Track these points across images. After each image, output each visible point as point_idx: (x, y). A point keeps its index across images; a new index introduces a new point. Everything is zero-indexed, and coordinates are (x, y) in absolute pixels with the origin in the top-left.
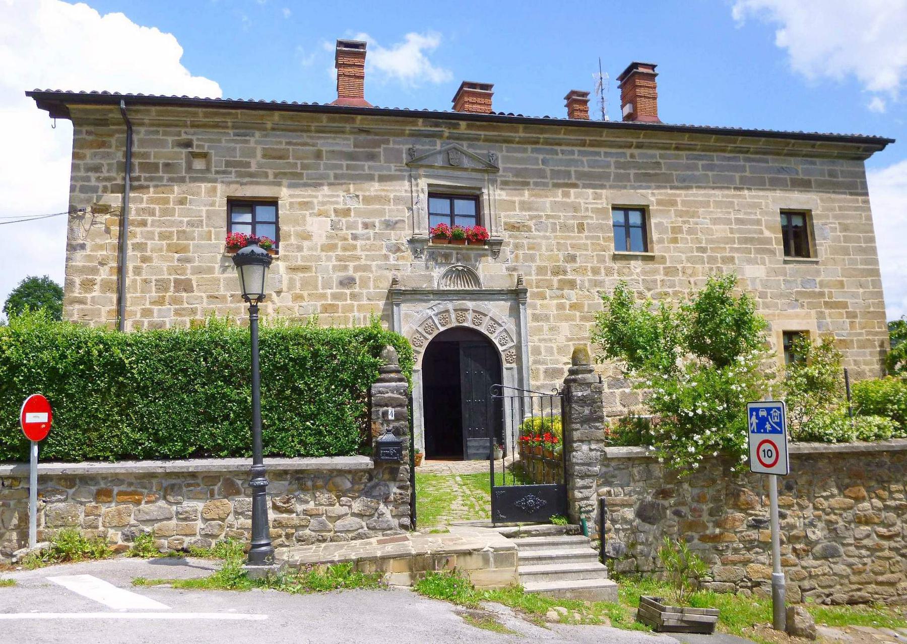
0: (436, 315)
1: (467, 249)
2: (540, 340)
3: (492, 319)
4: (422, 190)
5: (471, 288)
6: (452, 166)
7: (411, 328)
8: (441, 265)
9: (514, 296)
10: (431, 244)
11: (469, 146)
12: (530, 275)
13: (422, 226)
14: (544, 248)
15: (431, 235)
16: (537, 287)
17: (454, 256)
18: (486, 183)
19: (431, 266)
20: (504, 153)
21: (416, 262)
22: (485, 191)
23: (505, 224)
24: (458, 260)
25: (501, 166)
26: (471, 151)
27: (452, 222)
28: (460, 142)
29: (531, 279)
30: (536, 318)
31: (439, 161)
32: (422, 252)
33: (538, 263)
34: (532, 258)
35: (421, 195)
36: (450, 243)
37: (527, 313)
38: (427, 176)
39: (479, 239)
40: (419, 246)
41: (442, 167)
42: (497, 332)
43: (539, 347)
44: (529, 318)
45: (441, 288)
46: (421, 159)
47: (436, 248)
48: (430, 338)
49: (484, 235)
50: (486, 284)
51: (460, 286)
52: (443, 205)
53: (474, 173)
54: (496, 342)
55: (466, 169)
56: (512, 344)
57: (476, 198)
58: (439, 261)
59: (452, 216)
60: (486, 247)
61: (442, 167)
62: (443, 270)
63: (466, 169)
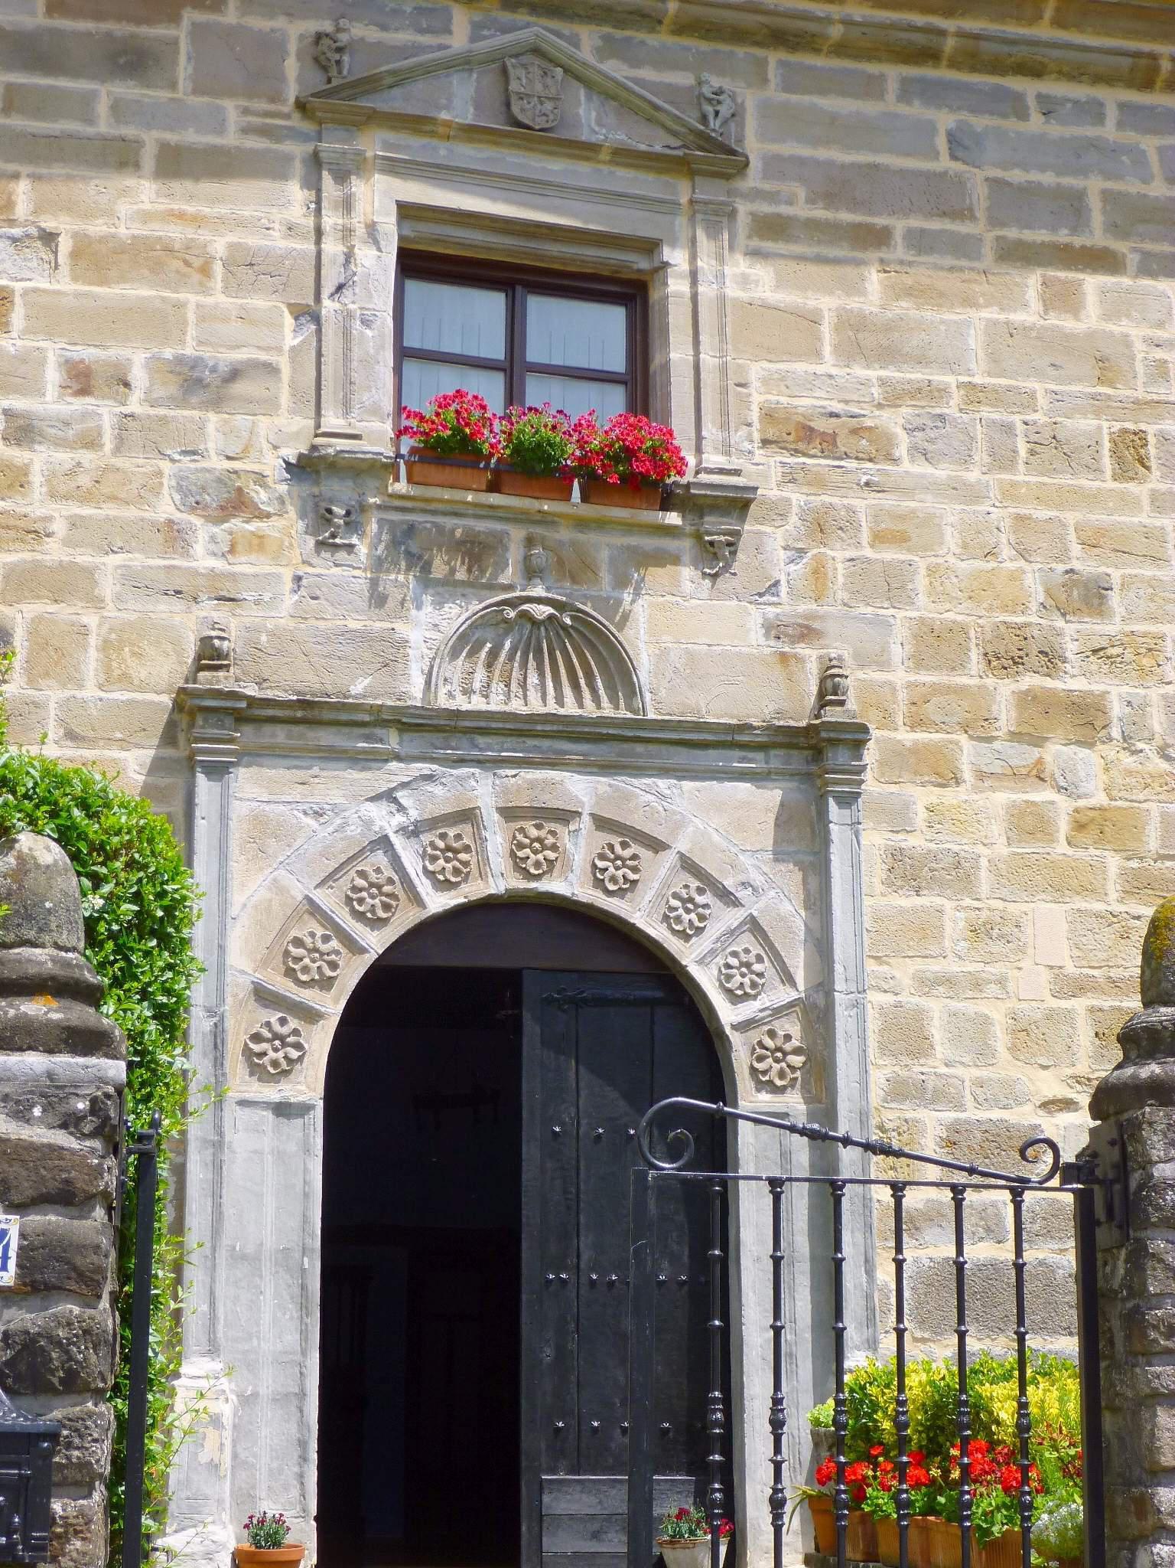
0: (412, 832)
1: (582, 524)
2: (927, 984)
3: (687, 864)
4: (372, 229)
5: (590, 710)
6: (518, 130)
7: (278, 887)
8: (447, 588)
9: (798, 760)
10: (402, 487)
11: (610, 48)
12: (884, 665)
13: (363, 397)
14: (951, 540)
15: (407, 444)
16: (917, 723)
17: (514, 554)
18: (681, 222)
19: (395, 595)
20: (773, 92)
21: (326, 569)
22: (676, 257)
23: (769, 415)
24: (531, 573)
25: (754, 146)
26: (615, 69)
27: (513, 394)
28: (565, 27)
29: (884, 683)
30: (907, 871)
31: (461, 101)
32: (353, 524)
33: (924, 607)
34: (893, 586)
35: (366, 255)
36: (494, 487)
37: (860, 845)
38: (394, 167)
39: (636, 474)
40: (340, 492)
41: (471, 133)
42: (714, 929)
43: (919, 1016)
44: (875, 872)
45: (443, 702)
46: (370, 84)
47: (427, 507)
48: (376, 942)
49: (665, 458)
50: (662, 695)
51: (535, 697)
53: (621, 172)
54: (706, 979)
55: (585, 150)
56: (784, 995)
58: (439, 569)
59: (514, 368)
60: (673, 518)
61: (471, 133)
62: (456, 615)
63: (585, 150)
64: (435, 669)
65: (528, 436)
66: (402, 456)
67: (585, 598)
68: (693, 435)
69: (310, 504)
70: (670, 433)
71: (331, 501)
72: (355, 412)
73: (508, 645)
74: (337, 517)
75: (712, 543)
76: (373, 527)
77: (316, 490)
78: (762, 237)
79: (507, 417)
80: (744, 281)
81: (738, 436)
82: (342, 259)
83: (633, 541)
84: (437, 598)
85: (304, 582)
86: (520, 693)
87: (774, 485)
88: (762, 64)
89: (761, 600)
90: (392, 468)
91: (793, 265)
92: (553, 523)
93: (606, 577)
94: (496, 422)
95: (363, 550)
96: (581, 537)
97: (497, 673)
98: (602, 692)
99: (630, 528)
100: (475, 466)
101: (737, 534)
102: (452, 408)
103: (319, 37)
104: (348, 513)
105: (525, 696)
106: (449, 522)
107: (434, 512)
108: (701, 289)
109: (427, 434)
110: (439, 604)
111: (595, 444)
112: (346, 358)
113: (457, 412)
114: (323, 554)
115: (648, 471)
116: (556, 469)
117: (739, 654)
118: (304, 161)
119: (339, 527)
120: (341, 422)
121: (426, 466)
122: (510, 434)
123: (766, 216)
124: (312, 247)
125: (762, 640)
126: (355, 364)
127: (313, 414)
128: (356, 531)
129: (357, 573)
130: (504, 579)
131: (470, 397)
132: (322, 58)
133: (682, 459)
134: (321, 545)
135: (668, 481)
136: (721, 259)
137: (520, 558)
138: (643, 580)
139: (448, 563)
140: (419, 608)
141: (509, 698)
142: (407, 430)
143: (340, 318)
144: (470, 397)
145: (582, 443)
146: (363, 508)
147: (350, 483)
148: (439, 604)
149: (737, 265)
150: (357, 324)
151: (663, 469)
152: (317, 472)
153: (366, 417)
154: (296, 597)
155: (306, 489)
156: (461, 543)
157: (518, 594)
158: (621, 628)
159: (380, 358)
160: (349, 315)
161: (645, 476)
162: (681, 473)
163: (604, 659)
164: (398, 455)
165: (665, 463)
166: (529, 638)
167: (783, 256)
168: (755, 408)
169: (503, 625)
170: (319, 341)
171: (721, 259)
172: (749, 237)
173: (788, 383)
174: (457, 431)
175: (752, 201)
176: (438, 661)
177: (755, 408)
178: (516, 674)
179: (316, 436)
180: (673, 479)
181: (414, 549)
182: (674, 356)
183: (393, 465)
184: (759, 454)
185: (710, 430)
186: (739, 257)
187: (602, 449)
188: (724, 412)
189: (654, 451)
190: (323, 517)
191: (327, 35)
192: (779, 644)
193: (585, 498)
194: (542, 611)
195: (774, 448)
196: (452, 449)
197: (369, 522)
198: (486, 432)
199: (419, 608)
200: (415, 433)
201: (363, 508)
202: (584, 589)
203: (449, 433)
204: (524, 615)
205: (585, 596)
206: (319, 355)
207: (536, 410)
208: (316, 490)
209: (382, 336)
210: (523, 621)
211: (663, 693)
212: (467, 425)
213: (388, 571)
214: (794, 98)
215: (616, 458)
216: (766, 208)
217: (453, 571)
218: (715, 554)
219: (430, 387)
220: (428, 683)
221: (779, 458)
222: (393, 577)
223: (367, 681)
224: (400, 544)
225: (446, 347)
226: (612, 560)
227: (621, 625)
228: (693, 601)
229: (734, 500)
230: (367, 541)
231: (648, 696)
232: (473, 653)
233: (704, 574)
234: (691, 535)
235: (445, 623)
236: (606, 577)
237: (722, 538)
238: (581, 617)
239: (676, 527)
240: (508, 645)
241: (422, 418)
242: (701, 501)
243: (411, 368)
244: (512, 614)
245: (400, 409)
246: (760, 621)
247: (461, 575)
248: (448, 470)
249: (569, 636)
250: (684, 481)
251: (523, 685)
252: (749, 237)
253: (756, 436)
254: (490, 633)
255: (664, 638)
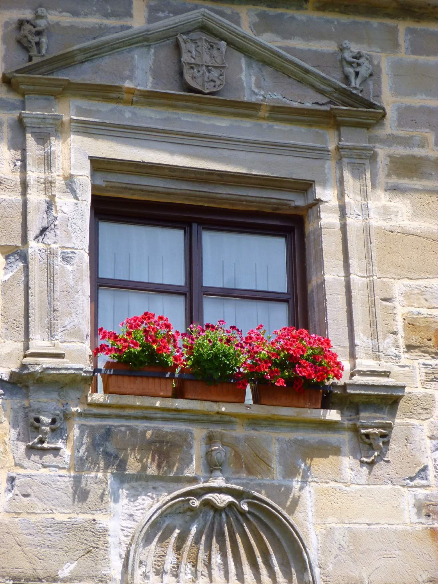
1: (254, 422)
4: (69, 181)
6: (190, 96)
8: (140, 483)
10: (99, 397)
11: (265, 24)
13: (65, 322)
15: (103, 359)
17: (197, 450)
18: (330, 165)
19: (95, 490)
20: (404, 55)
21: (36, 470)
22: (326, 194)
23: (411, 325)
24: (212, 466)
25: (389, 100)
26: (270, 40)
27: (193, 315)
28: (228, 9)
31: (142, 72)
32: (58, 430)
35: (64, 202)
36: (178, 393)
38: (86, 129)
39: (299, 381)
40: (47, 404)
41: (150, 98)
46: (65, 61)
47: (121, 412)
49: (324, 362)
52: (155, 253)
53: (278, 126)
55: (247, 109)
57: (289, 223)
58: (133, 467)
59: (192, 292)
60: (333, 415)
61: (150, 98)
62: (148, 505)
63: (247, 109)
64: (132, 554)
65: (206, 349)
66: (99, 371)
67: (260, 487)
68: (347, 343)
69: (21, 414)
70: (328, 342)
71: (39, 411)
72: (59, 335)
73: (194, 530)
74: (44, 425)
75: (367, 436)
76: (76, 432)
77: (26, 403)
78: (399, 176)
79: (188, 334)
80: (385, 212)
81: (386, 343)
82: (44, 206)
83: (300, 435)
84: (133, 492)
85: (17, 482)
86: (206, 572)
87: (418, 384)
88: (394, 31)
89: (412, 483)
90: (89, 381)
91: (426, 198)
92: (230, 422)
93: (277, 467)
94: (179, 339)
95: (66, 452)
96: (254, 433)
97: (185, 555)
98: (277, 568)
99: (297, 424)
100: (162, 377)
101: (389, 427)
102: (141, 328)
103: (21, 23)
104: (54, 421)
105: (210, 575)
106: (140, 425)
107: (128, 417)
108: (349, 221)
109: (120, 351)
110: (133, 497)
111: (264, 354)
112: (50, 289)
113: (146, 331)
114: (33, 457)
115: (310, 375)
116: (231, 376)
117: (395, 532)
118: (10, 126)
119: (46, 433)
120: (47, 343)
121: (120, 378)
122: (191, 348)
123: (402, 157)
124: (19, 198)
125: (415, 519)
126: (57, 295)
127: (22, 338)
128: (61, 437)
129: (63, 472)
130: (189, 473)
131: (156, 318)
132: (24, 40)
133: (339, 364)
134: (31, 449)
135: (328, 383)
136: (365, 196)
137: (202, 453)
138: (309, 469)
139: (140, 461)
140: (116, 500)
141: (196, 577)
142: (103, 348)
143: (44, 256)
144: (156, 318)
145: (252, 353)
146: (67, 416)
147: (55, 395)
148: (133, 497)
149: (379, 199)
150: (59, 261)
151: (324, 373)
152: (27, 387)
153: (67, 339)
154: (10, 495)
155: (17, 402)
156: (151, 442)
157: (201, 485)
158: (291, 511)
159: (79, 288)
160: (52, 254)
161: (307, 380)
162: (338, 376)
163: (278, 540)
164: (96, 370)
165: (324, 368)
166: (212, 524)
167: (417, 191)
168: (399, 319)
169: (189, 513)
170: (27, 276)
171: (365, 196)
172: (388, 175)
173: (427, 296)
174: (146, 347)
175: (389, 146)
176: (133, 546)
177: (399, 319)
178: (202, 555)
179: (25, 356)
180: (331, 381)
181: (111, 448)
182: (327, 277)
183: (91, 378)
184: (405, 358)
185: (361, 339)
186: (380, 193)
187: (270, 358)
188: (373, 323)
189: (314, 358)
190: (32, 425)
191: (28, 22)
192: (430, 522)
193: (256, 400)
194: (222, 500)
195: (417, 353)
196: (142, 363)
197: (71, 428)
198: (171, 347)
199: (116, 500)
200: (110, 350)
201: (67, 416)
202: (258, 479)
203: (139, 349)
204: (208, 504)
205: (260, 485)
206: (27, 287)
207: (213, 327)
208: (26, 403)
209: (80, 270)
210: (207, 509)
211: (330, 567)
212: (155, 341)
213: (89, 470)
214: (422, 59)
215: (282, 366)
216: (401, 151)
217: (144, 468)
218: (371, 445)
219: (121, 312)
220: (126, 566)
221: (422, 361)
222: (93, 474)
223: (73, 566)
224: (99, 445)
225: (135, 277)
226: (282, 452)
227: (292, 510)
228: (353, 486)
229: (384, 397)
230: (70, 444)
231: (317, 571)
232: (164, 538)
233: (362, 462)
234: (349, 429)
235: (139, 513)
236: (277, 467)
237: (376, 431)
238: (257, 505)
239: (336, 422)
240: (194, 530)
241: (115, 337)
242: (356, 400)
243: (106, 297)
244: (196, 503)
245: (97, 330)
246: (413, 501)
247: (152, 471)
248: (139, 380)
249: (247, 520)
250: (341, 382)
251: (208, 565)
252: (388, 175)
253: (402, 343)
254: (178, 520)
255: (330, 519)
